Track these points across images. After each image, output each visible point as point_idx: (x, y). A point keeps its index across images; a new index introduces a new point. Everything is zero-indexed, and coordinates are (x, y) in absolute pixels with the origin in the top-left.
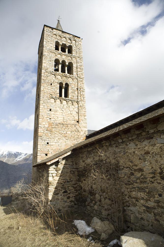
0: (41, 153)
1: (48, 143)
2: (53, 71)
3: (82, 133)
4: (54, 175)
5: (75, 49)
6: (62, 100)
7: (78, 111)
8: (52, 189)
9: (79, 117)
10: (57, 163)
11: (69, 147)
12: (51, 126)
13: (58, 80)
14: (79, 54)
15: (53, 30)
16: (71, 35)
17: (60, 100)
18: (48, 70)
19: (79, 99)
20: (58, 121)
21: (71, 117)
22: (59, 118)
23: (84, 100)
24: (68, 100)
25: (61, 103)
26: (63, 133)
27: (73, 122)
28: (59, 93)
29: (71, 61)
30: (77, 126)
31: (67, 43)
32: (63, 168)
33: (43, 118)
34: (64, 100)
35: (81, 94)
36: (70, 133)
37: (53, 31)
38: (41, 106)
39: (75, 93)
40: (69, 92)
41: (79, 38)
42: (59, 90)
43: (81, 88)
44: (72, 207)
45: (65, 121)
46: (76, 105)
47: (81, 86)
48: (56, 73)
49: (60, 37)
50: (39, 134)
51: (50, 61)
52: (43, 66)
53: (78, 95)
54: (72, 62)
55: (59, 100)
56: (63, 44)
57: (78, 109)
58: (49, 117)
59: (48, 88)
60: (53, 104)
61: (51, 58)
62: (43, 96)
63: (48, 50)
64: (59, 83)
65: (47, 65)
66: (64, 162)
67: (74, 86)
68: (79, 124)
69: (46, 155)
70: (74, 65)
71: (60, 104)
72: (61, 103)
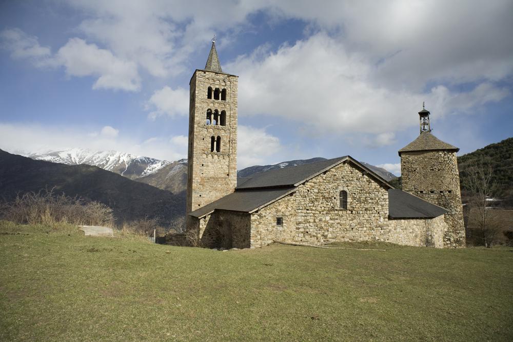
1: (200, 196)
4: (203, 224)
6: (213, 155)
8: (202, 232)
10: (205, 217)
15: (205, 73)
27: (223, 176)
29: (224, 109)
30: (227, 180)
32: (209, 220)
36: (220, 186)
38: (194, 163)
44: (214, 243)
54: (226, 110)
56: (216, 88)
66: (209, 216)
69: (199, 205)
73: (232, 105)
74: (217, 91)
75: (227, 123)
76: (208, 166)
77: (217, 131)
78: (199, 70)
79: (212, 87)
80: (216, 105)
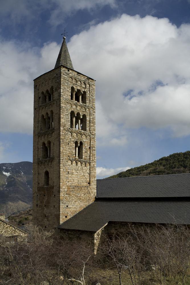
0: (62, 216)
1: (67, 206)
2: (70, 127)
3: (92, 195)
5: (89, 96)
7: (90, 172)
9: (90, 178)
13: (74, 138)
14: (92, 103)
17: (76, 162)
19: (91, 160)
22: (75, 181)
24: (82, 162)
25: (77, 165)
30: (89, 188)
33: (63, 182)
35: (93, 153)
38: (61, 170)
43: (93, 147)
49: (75, 81)
50: (61, 198)
51: (67, 115)
52: (61, 123)
53: (90, 155)
54: (86, 114)
57: (89, 170)
60: (70, 167)
61: (68, 110)
62: (62, 159)
65: (65, 120)
67: (87, 144)
68: (90, 185)
69: (66, 217)
70: (87, 119)
71: (76, 166)
72: (77, 165)
73: (91, 109)
74: (79, 91)
75: (88, 129)
76: (72, 174)
79: (75, 87)
80: (79, 108)
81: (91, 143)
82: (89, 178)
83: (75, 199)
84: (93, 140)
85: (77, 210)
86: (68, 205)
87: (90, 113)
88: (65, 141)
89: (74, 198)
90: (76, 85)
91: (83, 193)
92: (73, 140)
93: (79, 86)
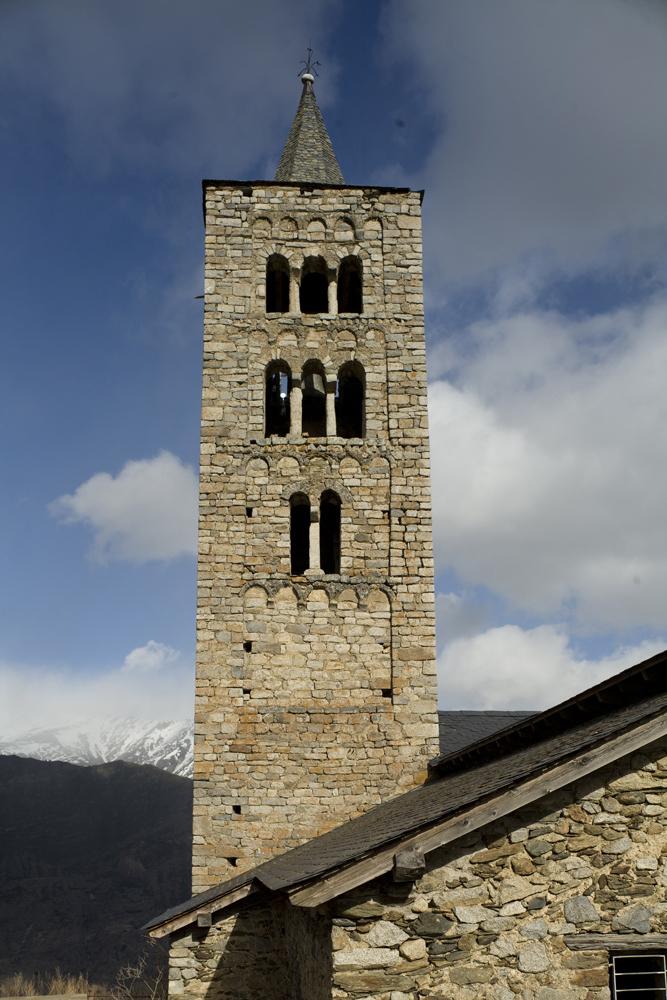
0: (207, 857)
1: (237, 809)
2: (260, 437)
3: (407, 752)
5: (376, 270)
6: (302, 590)
11: (340, 824)
12: (250, 728)
13: (284, 480)
14: (397, 299)
15: (249, 194)
16: (353, 192)
18: (228, 438)
19: (395, 571)
20: (286, 697)
21: (353, 671)
22: (291, 683)
23: (422, 572)
26: (307, 756)
27: (361, 698)
28: (288, 552)
30: (382, 719)
31: (330, 246)
33: (211, 690)
34: (316, 588)
35: (409, 537)
36: (342, 752)
37: (254, 199)
39: (377, 537)
40: (344, 536)
41: (405, 191)
42: (287, 536)
43: (406, 505)
45: (323, 694)
46: (379, 607)
47: (408, 491)
48: (272, 445)
49: (290, 225)
51: (240, 383)
54: (362, 357)
55: (289, 589)
56: (308, 261)
57: (387, 624)
58: (240, 683)
59: (231, 535)
61: (243, 364)
63: (230, 322)
64: (287, 497)
65: (228, 409)
70: (369, 378)
71: (296, 613)
73: (395, 333)
75: (372, 424)
76: (275, 649)
77: (317, 467)
78: (219, 184)
79: (287, 253)
80: (313, 340)
81: (397, 490)
82: (387, 664)
83: (285, 774)
84: (407, 472)
85: (299, 831)
86: (241, 802)
87: (387, 349)
88: (226, 502)
89: (279, 771)
90: (300, 241)
91: (343, 745)
92: (280, 489)
93: (316, 242)
